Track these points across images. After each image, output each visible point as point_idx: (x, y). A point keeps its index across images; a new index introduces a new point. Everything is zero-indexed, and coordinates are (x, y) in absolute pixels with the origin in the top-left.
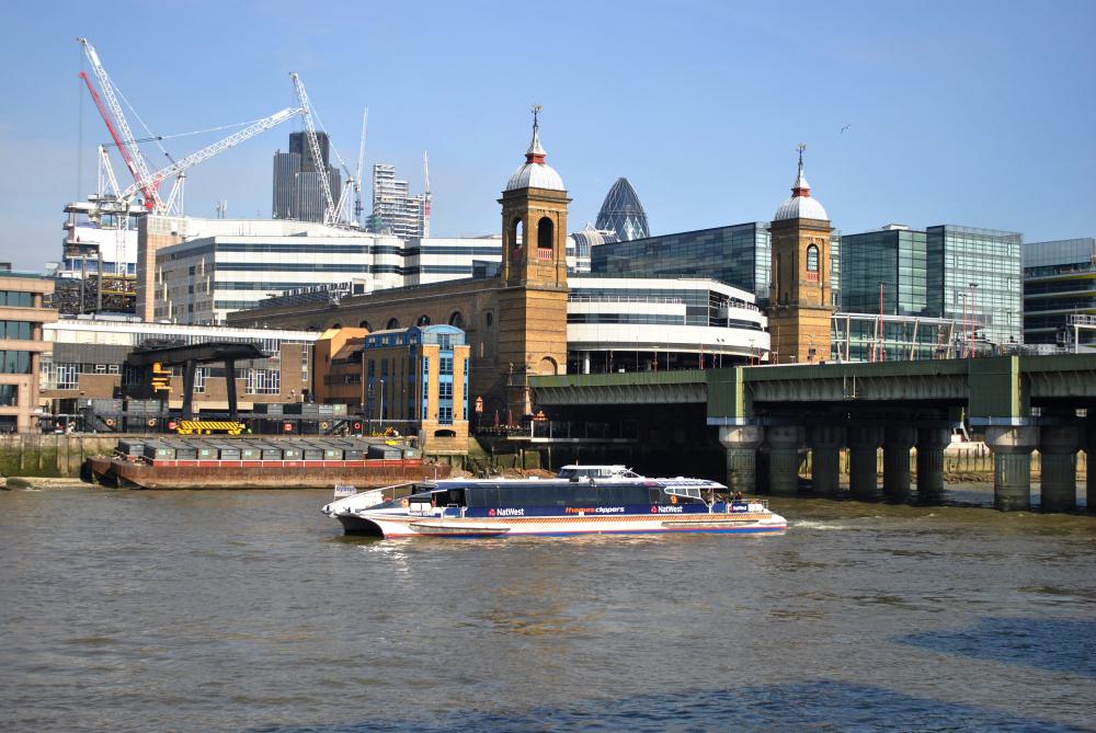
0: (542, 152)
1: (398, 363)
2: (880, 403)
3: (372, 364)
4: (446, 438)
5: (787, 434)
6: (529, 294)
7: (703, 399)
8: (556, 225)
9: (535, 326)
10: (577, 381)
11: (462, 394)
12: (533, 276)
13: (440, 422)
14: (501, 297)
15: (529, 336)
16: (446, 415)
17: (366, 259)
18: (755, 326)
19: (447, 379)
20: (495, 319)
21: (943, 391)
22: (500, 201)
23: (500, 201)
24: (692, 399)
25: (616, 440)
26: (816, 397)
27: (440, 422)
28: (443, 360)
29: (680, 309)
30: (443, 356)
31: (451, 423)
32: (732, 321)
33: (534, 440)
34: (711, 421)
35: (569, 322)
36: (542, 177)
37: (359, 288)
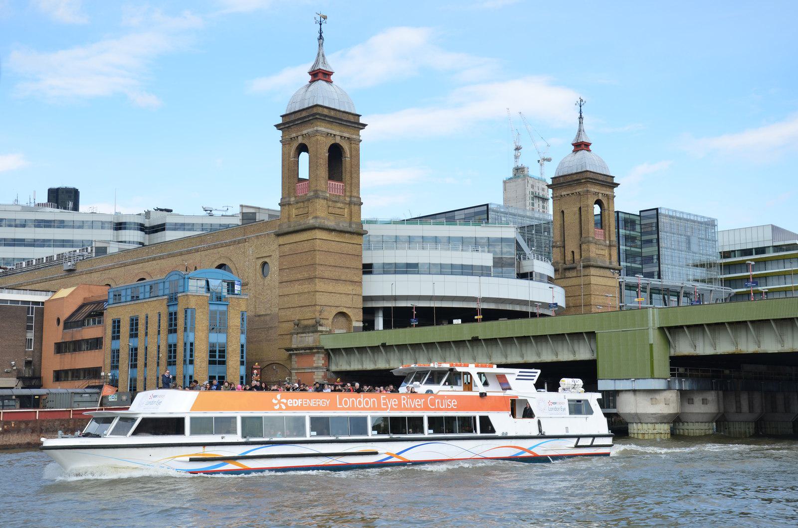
3: (117, 324)
5: (705, 401)
8: (348, 154)
9: (326, 274)
11: (239, 359)
14: (282, 240)
19: (218, 338)
20: (274, 266)
22: (277, 126)
23: (277, 126)
37: (101, 251)
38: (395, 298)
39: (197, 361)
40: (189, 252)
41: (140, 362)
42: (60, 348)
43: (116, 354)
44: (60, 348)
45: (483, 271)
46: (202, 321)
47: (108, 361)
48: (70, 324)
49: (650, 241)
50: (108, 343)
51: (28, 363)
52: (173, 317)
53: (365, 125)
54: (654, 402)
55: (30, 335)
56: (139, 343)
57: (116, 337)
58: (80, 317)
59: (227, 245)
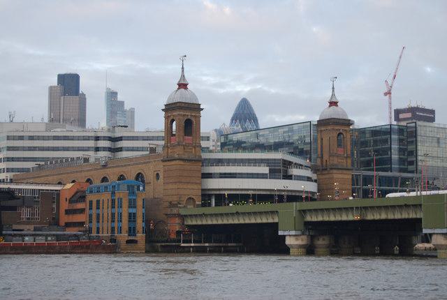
1: (106, 202)
2: (374, 221)
3: (91, 202)
4: (132, 244)
5: (324, 240)
7: (276, 220)
10: (207, 210)
13: (129, 235)
14: (165, 163)
16: (132, 231)
17: (91, 143)
18: (309, 179)
20: (161, 177)
21: (409, 214)
22: (163, 110)
23: (163, 110)
24: (270, 221)
25: (229, 244)
26: (338, 218)
27: (129, 235)
28: (130, 200)
29: (265, 170)
33: (182, 245)
34: (280, 233)
35: (202, 178)
37: (86, 160)
38: (219, 190)
39: (123, 221)
40: (125, 166)
41: (101, 221)
42: (68, 212)
43: (90, 216)
44: (68, 212)
45: (263, 176)
46: (125, 204)
47: (88, 219)
48: (71, 201)
49: (412, 142)
50: (87, 210)
51: (53, 219)
52: (113, 201)
53: (202, 109)
54: (297, 240)
55: (54, 206)
56: (100, 211)
57: (91, 209)
58: (75, 198)
59: (142, 163)
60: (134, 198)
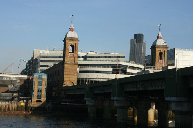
0: (73, 28)
4: (39, 103)
6: (65, 65)
8: (75, 47)
11: (44, 91)
12: (67, 60)
13: (37, 98)
15: (65, 76)
27: (37, 98)
28: (39, 82)
29: (111, 69)
30: (39, 81)
31: (41, 98)
32: (128, 73)
33: (62, 104)
36: (71, 34)
60: (41, 81)
